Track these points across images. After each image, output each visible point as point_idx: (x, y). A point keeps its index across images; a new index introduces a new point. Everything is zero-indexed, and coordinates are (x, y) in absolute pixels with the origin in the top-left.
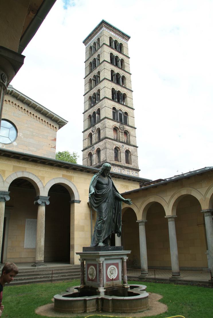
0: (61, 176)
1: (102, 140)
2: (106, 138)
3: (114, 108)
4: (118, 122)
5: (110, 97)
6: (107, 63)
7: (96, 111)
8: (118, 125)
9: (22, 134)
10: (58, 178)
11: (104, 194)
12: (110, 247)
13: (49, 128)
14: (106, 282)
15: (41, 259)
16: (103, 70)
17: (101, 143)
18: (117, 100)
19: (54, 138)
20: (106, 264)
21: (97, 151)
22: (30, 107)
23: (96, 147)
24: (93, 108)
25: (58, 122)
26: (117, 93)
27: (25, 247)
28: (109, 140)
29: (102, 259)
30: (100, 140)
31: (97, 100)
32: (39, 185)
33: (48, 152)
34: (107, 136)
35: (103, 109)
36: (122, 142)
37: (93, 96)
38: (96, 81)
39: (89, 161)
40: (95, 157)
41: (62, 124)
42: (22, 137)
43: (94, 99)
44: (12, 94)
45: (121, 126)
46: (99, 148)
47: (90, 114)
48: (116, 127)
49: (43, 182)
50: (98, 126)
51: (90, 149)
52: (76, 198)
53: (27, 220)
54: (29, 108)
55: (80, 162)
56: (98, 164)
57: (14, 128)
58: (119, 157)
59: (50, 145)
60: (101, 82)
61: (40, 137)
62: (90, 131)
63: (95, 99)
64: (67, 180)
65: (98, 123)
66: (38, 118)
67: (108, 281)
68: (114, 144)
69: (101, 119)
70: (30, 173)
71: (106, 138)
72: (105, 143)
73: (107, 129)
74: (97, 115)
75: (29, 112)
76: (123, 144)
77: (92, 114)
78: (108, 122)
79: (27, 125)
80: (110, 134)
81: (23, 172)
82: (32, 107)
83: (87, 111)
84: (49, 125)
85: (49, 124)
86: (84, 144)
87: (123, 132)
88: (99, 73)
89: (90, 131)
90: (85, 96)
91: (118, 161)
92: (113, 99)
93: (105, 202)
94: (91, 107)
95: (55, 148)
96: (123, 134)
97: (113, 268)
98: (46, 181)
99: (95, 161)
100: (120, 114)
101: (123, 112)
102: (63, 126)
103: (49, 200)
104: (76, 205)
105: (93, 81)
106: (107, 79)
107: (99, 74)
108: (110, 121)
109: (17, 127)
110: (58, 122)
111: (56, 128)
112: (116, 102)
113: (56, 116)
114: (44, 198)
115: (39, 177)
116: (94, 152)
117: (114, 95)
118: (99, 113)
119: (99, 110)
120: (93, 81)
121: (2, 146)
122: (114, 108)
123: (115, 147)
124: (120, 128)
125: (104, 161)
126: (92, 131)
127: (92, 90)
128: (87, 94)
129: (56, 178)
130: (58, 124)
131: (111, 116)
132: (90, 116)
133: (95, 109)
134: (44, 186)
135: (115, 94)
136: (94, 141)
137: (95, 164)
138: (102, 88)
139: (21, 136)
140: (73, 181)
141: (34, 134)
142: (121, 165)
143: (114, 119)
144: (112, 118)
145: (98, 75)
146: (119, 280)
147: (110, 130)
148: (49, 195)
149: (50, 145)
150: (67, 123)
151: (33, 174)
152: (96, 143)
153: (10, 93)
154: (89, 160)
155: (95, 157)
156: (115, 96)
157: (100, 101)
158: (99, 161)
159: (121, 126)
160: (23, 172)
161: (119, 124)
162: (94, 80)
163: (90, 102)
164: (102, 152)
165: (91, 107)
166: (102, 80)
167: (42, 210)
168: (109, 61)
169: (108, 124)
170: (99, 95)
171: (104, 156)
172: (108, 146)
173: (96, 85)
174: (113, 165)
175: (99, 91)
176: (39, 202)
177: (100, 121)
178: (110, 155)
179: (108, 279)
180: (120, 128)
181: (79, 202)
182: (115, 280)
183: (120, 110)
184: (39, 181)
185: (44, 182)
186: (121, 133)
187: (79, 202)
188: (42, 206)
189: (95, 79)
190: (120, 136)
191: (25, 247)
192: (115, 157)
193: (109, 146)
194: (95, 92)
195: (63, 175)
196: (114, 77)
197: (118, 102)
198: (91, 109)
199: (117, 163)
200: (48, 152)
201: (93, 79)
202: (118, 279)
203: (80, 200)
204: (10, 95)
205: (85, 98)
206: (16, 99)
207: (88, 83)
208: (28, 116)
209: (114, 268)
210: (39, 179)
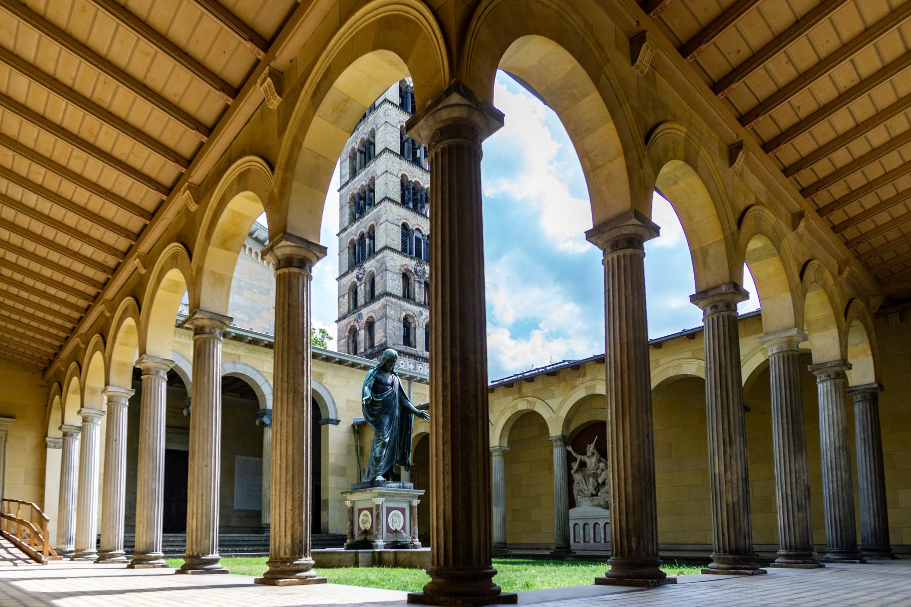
1: (379, 298)
2: (388, 294)
3: (405, 226)
4: (411, 258)
5: (397, 197)
6: (391, 107)
7: (365, 231)
8: (411, 264)
16: (383, 127)
17: (376, 306)
18: (411, 205)
21: (367, 322)
23: (366, 312)
24: (359, 223)
26: (414, 188)
28: (393, 300)
30: (372, 297)
31: (370, 205)
34: (389, 290)
35: (381, 227)
36: (419, 305)
37: (359, 194)
38: (365, 154)
39: (351, 345)
40: (362, 335)
43: (362, 202)
45: (419, 268)
46: (371, 317)
47: (352, 237)
48: (408, 270)
50: (370, 265)
51: (352, 318)
55: (332, 346)
56: (369, 351)
58: (412, 338)
60: (375, 157)
62: (352, 277)
63: (365, 200)
65: (369, 259)
68: (403, 310)
69: (376, 250)
71: (388, 294)
72: (385, 306)
73: (389, 275)
74: (367, 240)
76: (421, 309)
77: (356, 238)
78: (392, 259)
80: (395, 284)
83: (345, 230)
86: (339, 307)
87: (423, 281)
88: (373, 134)
89: (352, 277)
90: (343, 191)
91: (410, 346)
92: (404, 203)
94: (353, 220)
96: (423, 286)
99: (363, 345)
100: (418, 240)
101: (423, 236)
105: (358, 154)
106: (391, 151)
107: (374, 137)
108: (396, 256)
112: (408, 208)
116: (361, 325)
117: (406, 192)
118: (372, 237)
119: (372, 230)
120: (358, 154)
122: (405, 226)
123: (404, 314)
124: (416, 272)
125: (381, 345)
126: (358, 278)
127: (356, 179)
128: (346, 188)
131: (397, 244)
132: (352, 241)
133: (363, 225)
135: (409, 190)
136: (361, 300)
137: (362, 350)
138: (379, 173)
142: (414, 353)
143: (405, 251)
144: (400, 250)
145: (371, 140)
147: (395, 276)
152: (366, 305)
154: (351, 341)
155: (362, 335)
156: (409, 193)
157: (375, 206)
158: (372, 346)
159: (419, 268)
161: (414, 263)
162: (361, 152)
163: (354, 209)
164: (378, 326)
165: (353, 220)
166: (380, 154)
168: (397, 101)
169: (392, 263)
170: (372, 190)
171: (383, 334)
172: (390, 312)
173: (364, 165)
174: (400, 352)
175: (373, 181)
177: (373, 253)
178: (394, 333)
180: (416, 272)
183: (418, 229)
186: (417, 285)
189: (363, 149)
190: (417, 290)
192: (404, 336)
193: (392, 312)
194: (364, 183)
196: (406, 144)
197: (415, 209)
198: (355, 226)
199: (409, 350)
201: (359, 150)
205: (341, 196)
207: (348, 160)
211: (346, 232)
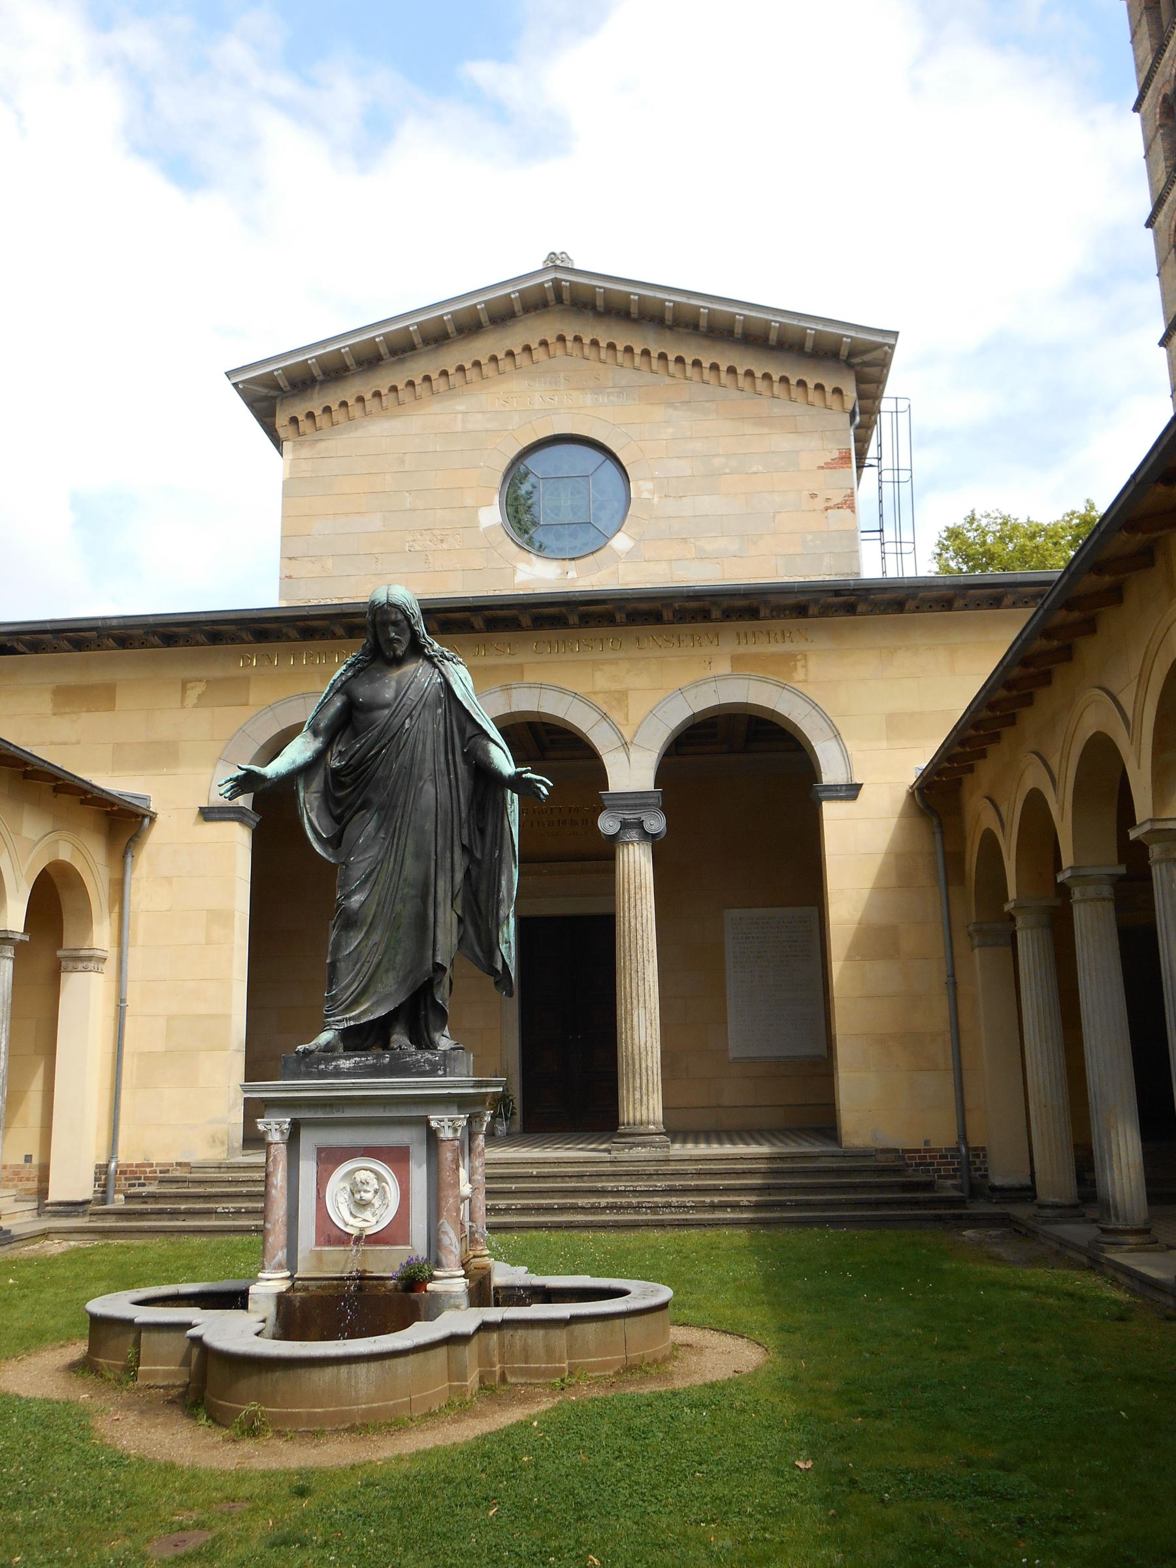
0: (724, 667)
9: (650, 485)
10: (705, 681)
11: (360, 763)
12: (348, 1058)
13: (799, 408)
14: (318, 1244)
15: (644, 1118)
19: (836, 455)
20: (320, 1151)
22: (670, 328)
25: (844, 352)
27: (732, 1054)
29: (272, 1120)
32: (600, 738)
33: (809, 537)
41: (867, 358)
42: (656, 500)
44: (566, 296)
49: (616, 716)
52: (831, 773)
53: (732, 914)
54: (668, 333)
57: (609, 466)
59: (813, 496)
61: (754, 469)
64: (765, 680)
66: (723, 375)
67: (329, 1242)
70: (541, 687)
75: (671, 357)
79: (670, 430)
81: (507, 688)
82: (687, 326)
84: (796, 392)
85: (793, 381)
93: (366, 805)
95: (852, 508)
97: (362, 1175)
98: (638, 707)
102: (884, 364)
103: (666, 809)
104: (831, 811)
109: (619, 455)
110: (844, 352)
111: (838, 391)
113: (820, 327)
114: (631, 802)
115: (593, 698)
121: (559, 571)
129: (696, 684)
130: (850, 366)
134: (628, 740)
139: (646, 495)
140: (805, 681)
141: (717, 462)
146: (407, 1243)
148: (658, 782)
149: (813, 496)
150: (892, 347)
151: (562, 691)
153: (551, 296)
160: (507, 688)
167: (637, 864)
176: (607, 824)
179: (331, 1235)
181: (851, 791)
182: (375, 1239)
184: (595, 716)
185: (627, 715)
187: (851, 791)
188: (627, 843)
191: (732, 1054)
195: (736, 661)
200: (809, 537)
202: (405, 1239)
203: (857, 781)
204: (560, 307)
206: (591, 314)
208: (668, 380)
209: (379, 1177)
210: (596, 708)
211: (1165, 207)
